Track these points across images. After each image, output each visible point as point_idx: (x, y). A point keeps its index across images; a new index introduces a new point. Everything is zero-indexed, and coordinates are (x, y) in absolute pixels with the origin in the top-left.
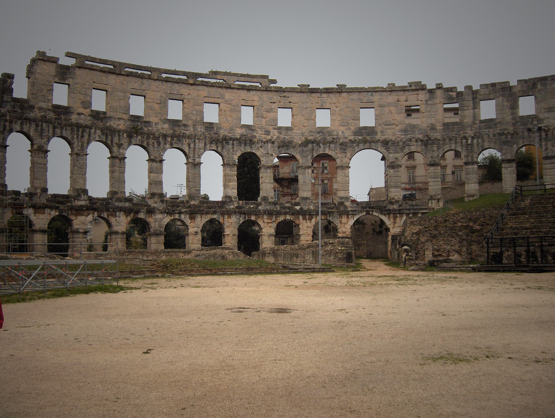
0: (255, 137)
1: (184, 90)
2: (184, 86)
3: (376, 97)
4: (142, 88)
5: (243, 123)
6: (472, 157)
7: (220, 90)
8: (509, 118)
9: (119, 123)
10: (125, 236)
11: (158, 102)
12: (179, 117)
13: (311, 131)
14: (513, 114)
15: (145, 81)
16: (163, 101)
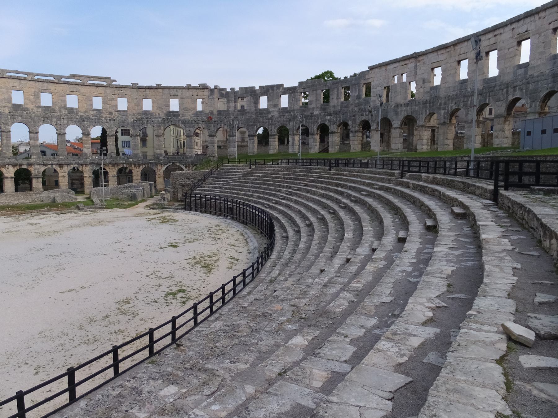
0: (102, 117)
1: (52, 87)
2: (51, 84)
3: (180, 92)
4: (20, 86)
5: (94, 107)
6: (233, 132)
7: (77, 86)
8: (253, 109)
9: (4, 109)
10: (13, 179)
11: (33, 95)
12: (50, 104)
13: (139, 113)
14: (255, 107)
15: (22, 81)
16: (36, 94)
